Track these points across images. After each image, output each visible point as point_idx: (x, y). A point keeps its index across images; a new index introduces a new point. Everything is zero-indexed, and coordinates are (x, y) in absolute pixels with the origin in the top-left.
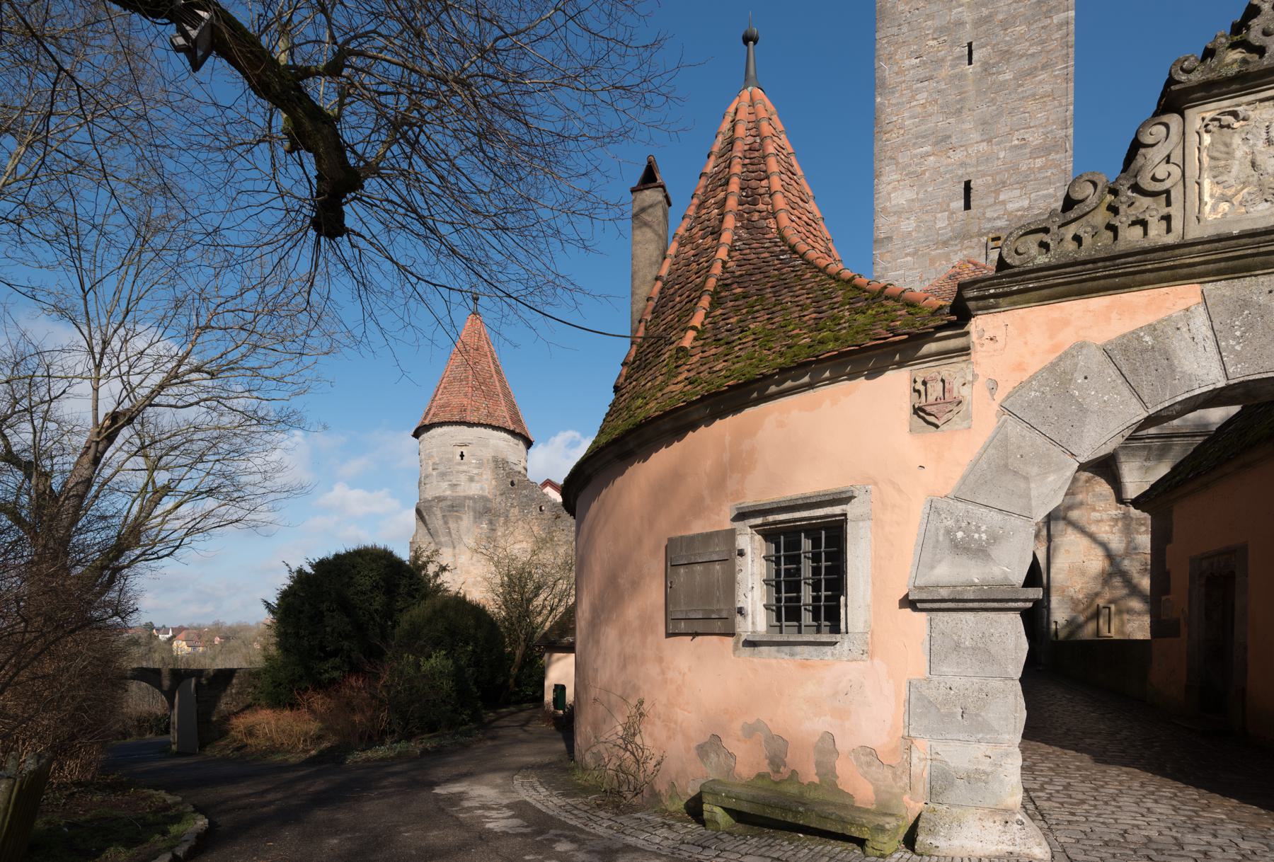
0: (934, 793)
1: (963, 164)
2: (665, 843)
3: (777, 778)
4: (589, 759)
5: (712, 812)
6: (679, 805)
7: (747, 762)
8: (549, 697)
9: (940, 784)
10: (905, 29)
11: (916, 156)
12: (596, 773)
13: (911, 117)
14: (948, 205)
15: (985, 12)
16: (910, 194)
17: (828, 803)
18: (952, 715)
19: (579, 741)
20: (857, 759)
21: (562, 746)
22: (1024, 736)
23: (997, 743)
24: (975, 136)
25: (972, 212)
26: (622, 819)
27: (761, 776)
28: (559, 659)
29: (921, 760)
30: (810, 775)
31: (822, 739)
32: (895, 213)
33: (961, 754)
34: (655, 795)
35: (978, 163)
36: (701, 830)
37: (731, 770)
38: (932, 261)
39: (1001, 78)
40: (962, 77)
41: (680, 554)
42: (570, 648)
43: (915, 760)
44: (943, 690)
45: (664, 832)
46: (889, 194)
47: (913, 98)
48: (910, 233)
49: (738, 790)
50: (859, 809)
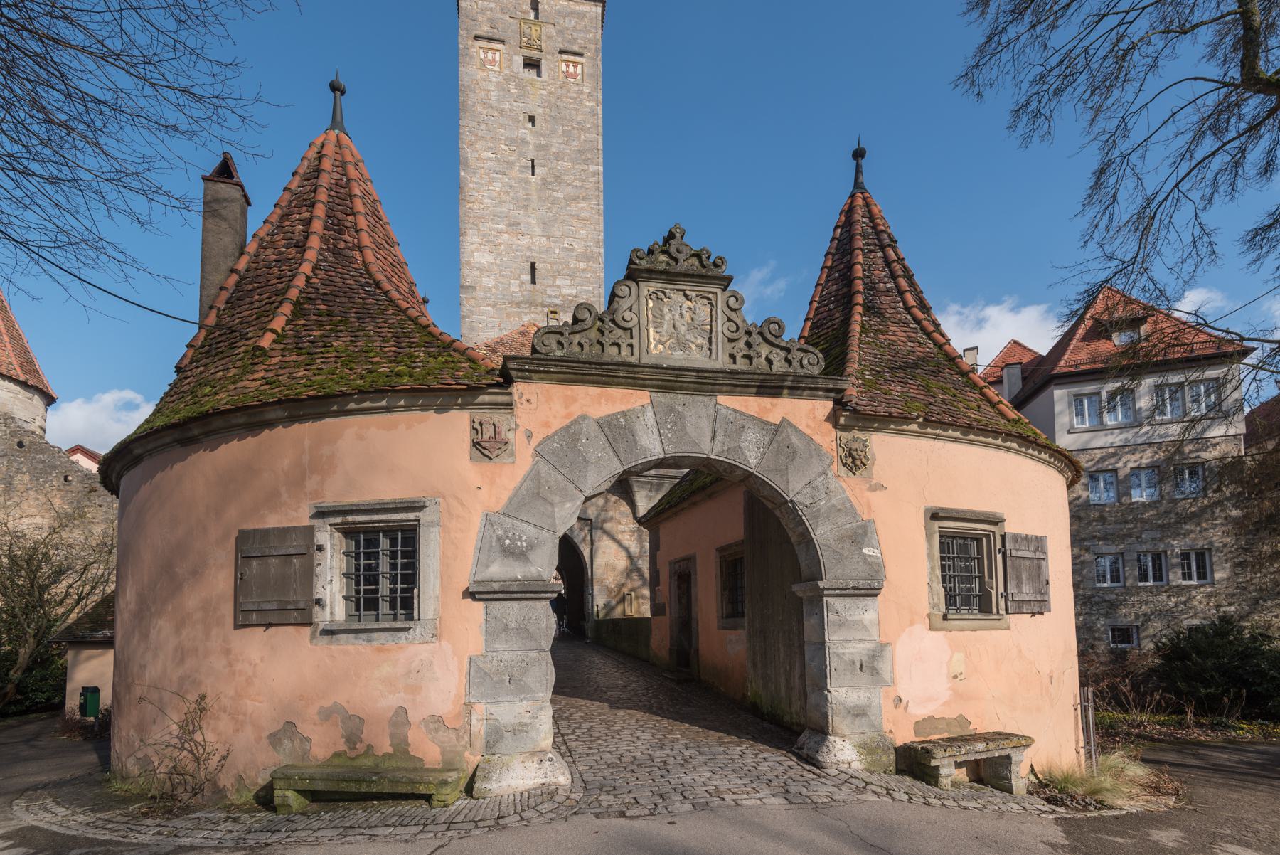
0: (489, 746)
1: (529, 248)
2: (229, 836)
3: (353, 754)
4: (132, 767)
5: (284, 796)
6: (248, 796)
7: (322, 744)
8: (73, 702)
9: (494, 738)
12: (141, 780)
17: (399, 769)
18: (502, 682)
19: (117, 747)
20: (426, 727)
21: (93, 758)
22: (554, 693)
23: (534, 700)
24: (538, 231)
25: (537, 286)
26: (178, 823)
27: (337, 755)
28: (90, 658)
29: (479, 721)
30: (385, 746)
31: (396, 713)
33: (509, 712)
34: (219, 792)
35: (540, 252)
36: (272, 816)
37: (306, 753)
38: (508, 315)
41: (251, 546)
42: (108, 643)
43: (474, 722)
44: (495, 663)
45: (229, 826)
49: (311, 771)
50: (428, 769)
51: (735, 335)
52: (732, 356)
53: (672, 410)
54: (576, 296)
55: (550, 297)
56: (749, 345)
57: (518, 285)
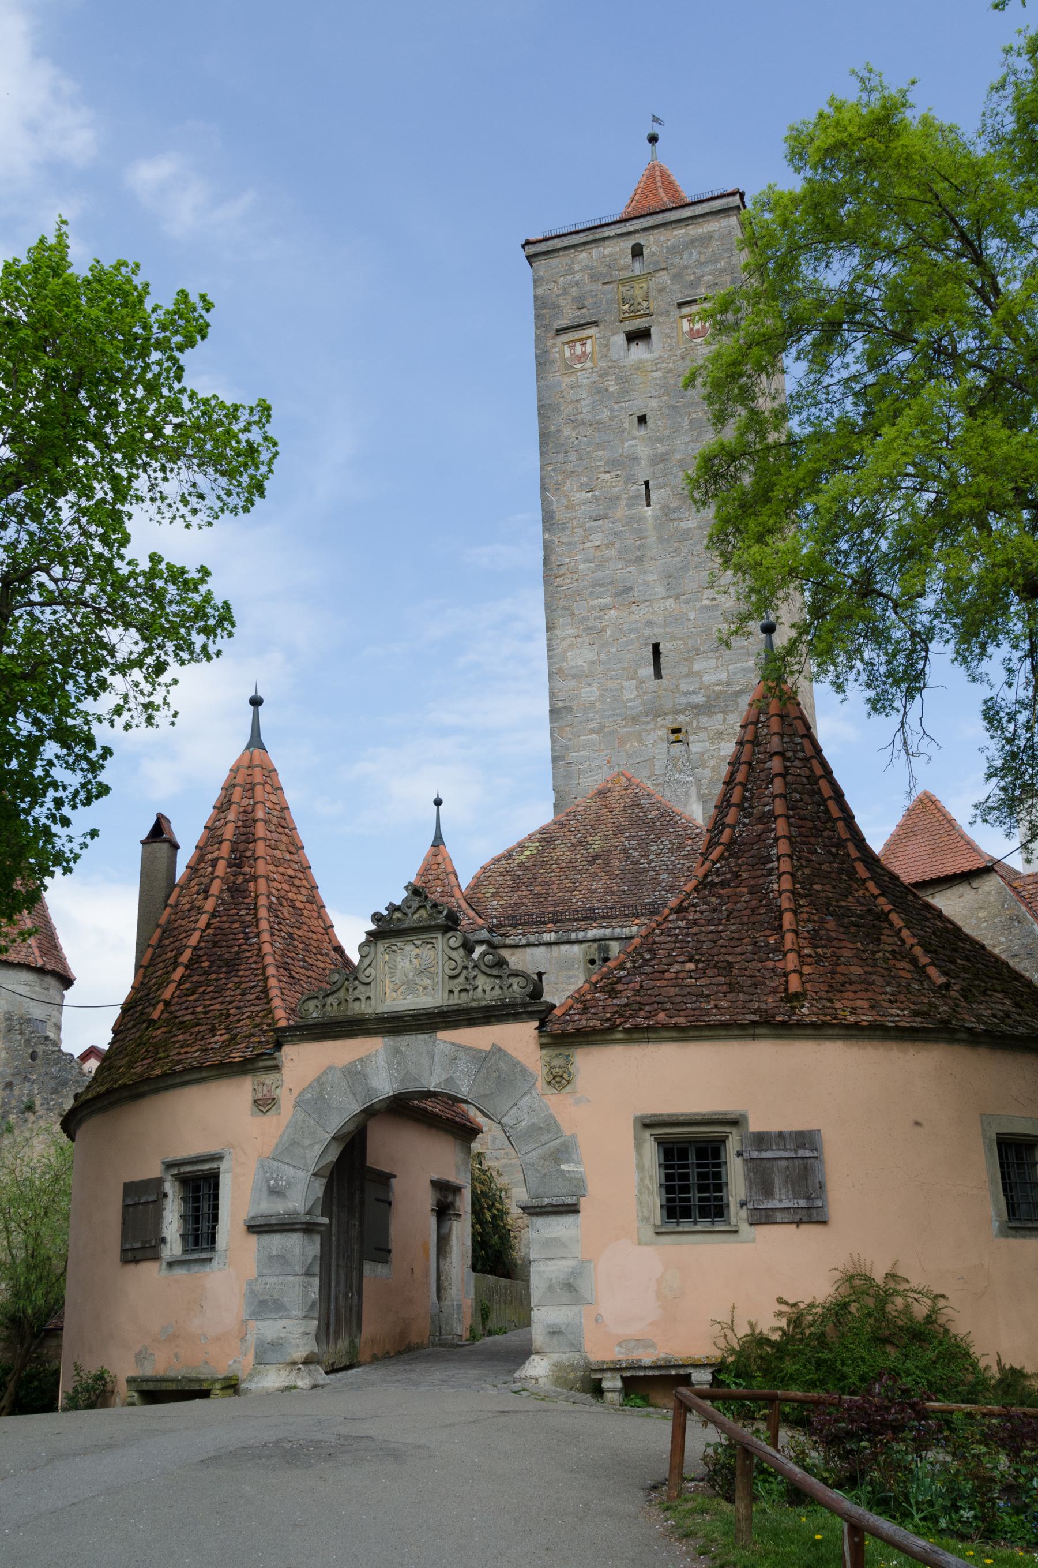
1: (649, 623)
10: (573, 457)
11: (594, 608)
13: (587, 561)
14: (636, 672)
15: (661, 449)
16: (589, 655)
24: (661, 590)
25: (664, 681)
32: (574, 677)
35: (666, 624)
39: (684, 525)
40: (641, 520)
46: (565, 651)
47: (586, 538)
48: (593, 703)
51: (454, 973)
52: (451, 992)
53: (397, 1051)
54: (727, 684)
55: (685, 694)
56: (467, 979)
57: (635, 686)
